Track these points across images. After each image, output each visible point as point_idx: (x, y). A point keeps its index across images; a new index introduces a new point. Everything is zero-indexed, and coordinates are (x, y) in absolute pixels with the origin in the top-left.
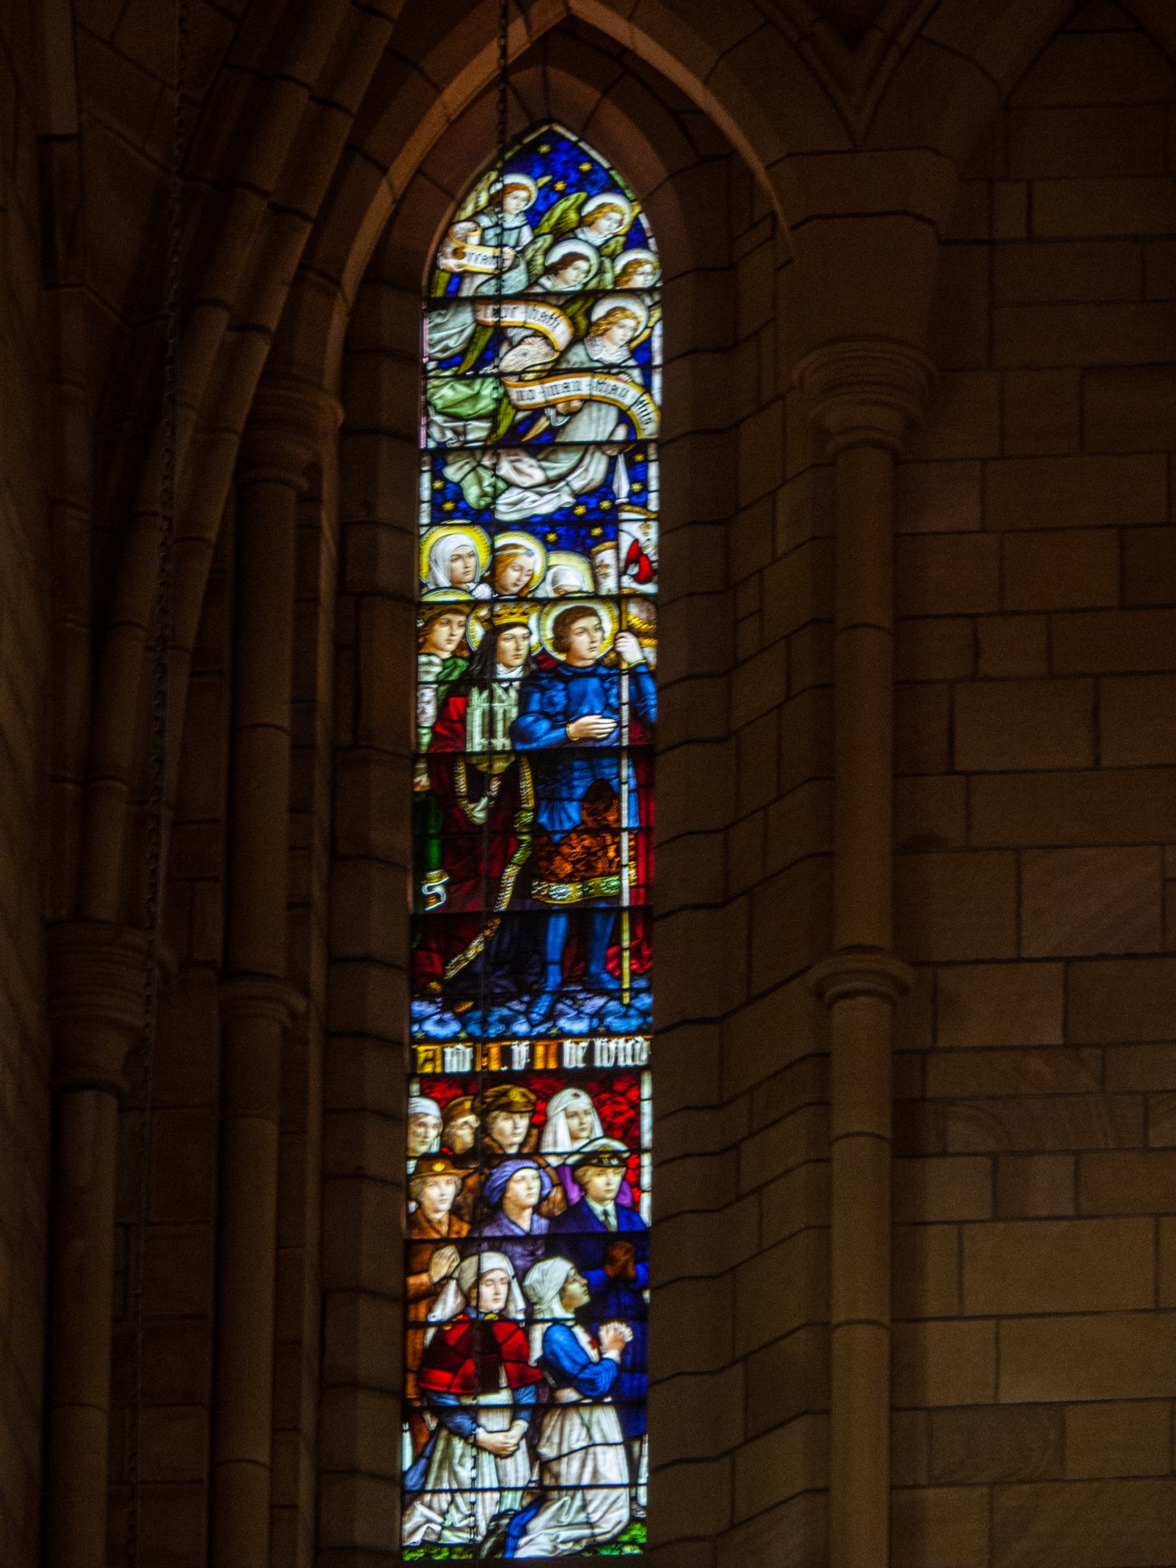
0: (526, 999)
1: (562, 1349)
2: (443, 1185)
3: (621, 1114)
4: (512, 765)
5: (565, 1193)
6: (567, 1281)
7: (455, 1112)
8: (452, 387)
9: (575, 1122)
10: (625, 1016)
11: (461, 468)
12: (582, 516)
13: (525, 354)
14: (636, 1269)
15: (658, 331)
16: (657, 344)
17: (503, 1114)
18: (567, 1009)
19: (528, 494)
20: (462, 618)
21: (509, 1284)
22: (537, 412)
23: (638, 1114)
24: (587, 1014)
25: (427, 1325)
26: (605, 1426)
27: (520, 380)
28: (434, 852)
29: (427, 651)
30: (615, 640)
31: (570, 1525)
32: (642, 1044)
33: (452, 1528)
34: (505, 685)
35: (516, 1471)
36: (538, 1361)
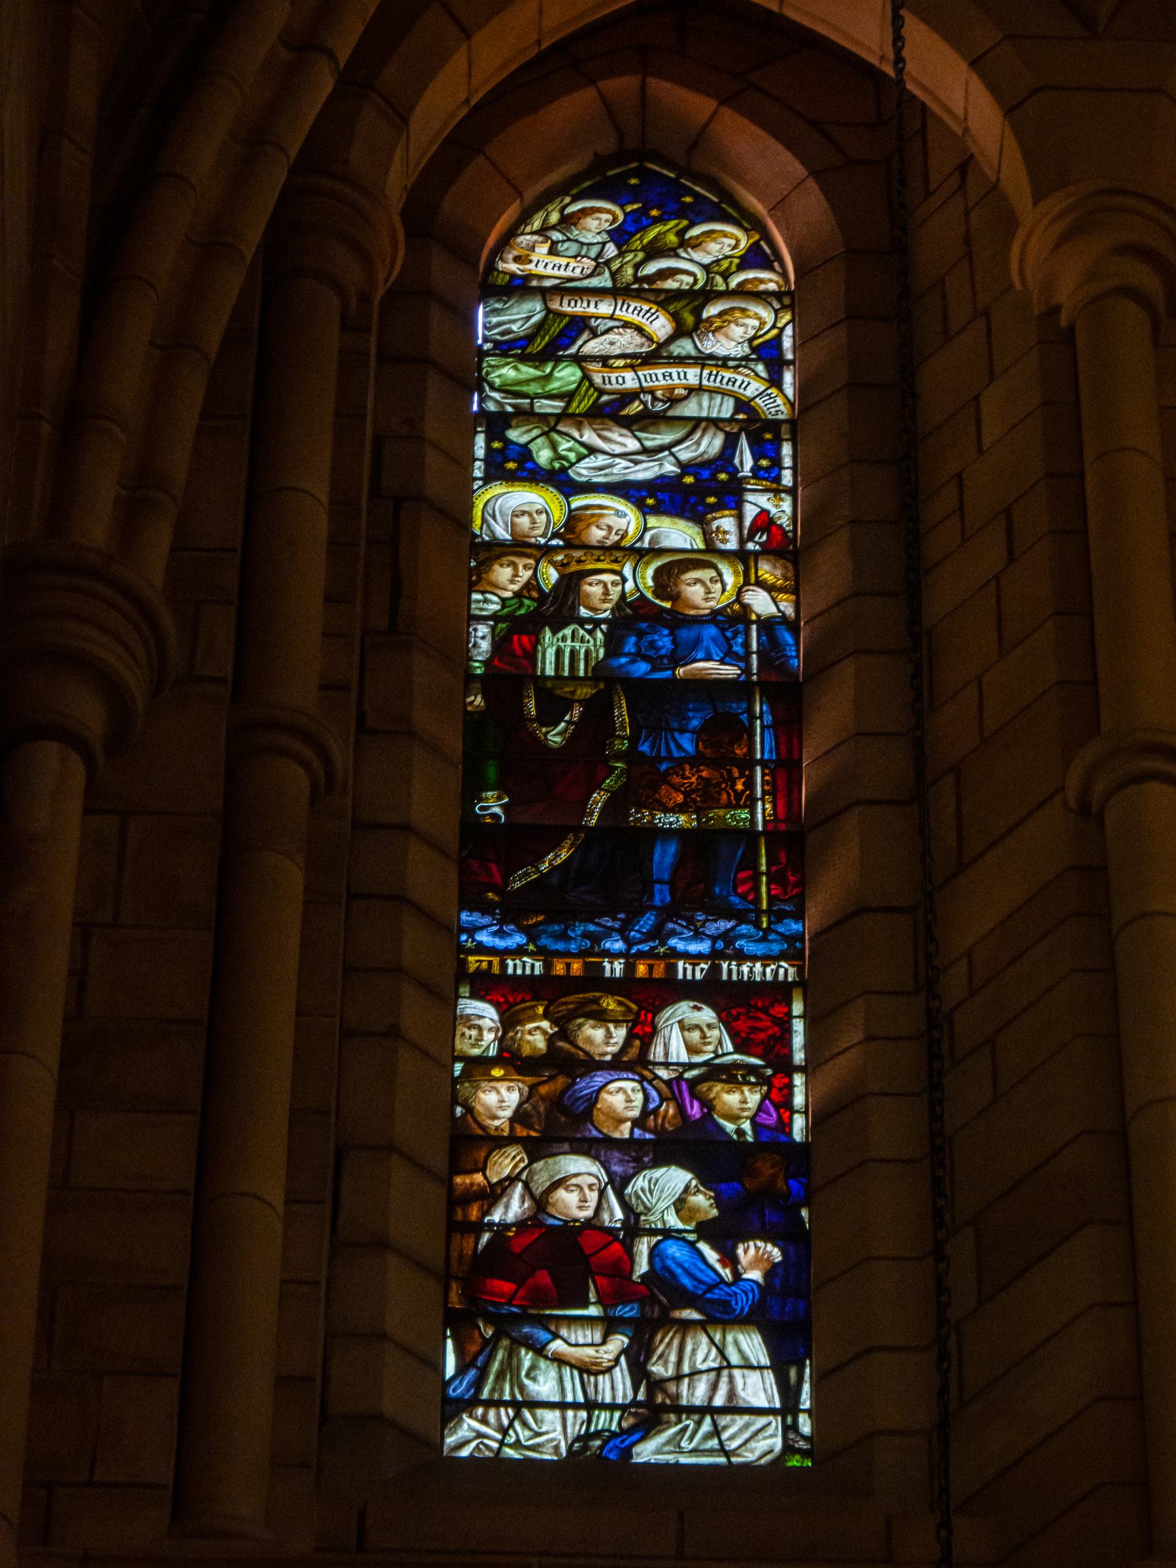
0: (622, 916)
1: (680, 1265)
2: (503, 1091)
3: (760, 1030)
4: (600, 692)
5: (681, 1109)
6: (687, 1189)
7: (521, 1017)
8: (515, 368)
9: (695, 1036)
10: (764, 939)
11: (529, 431)
12: (691, 485)
13: (612, 343)
14: (787, 1184)
15: (789, 331)
16: (787, 343)
17: (591, 1022)
18: (679, 929)
19: (618, 460)
20: (532, 561)
21: (602, 1193)
22: (629, 397)
23: (788, 1032)
24: (709, 936)
25: (479, 1227)
26: (744, 1346)
27: (604, 365)
28: (492, 772)
29: (481, 589)
30: (739, 592)
31: (694, 1451)
32: (786, 970)
33: (517, 1445)
34: (589, 627)
35: (613, 1388)
36: (642, 1277)
